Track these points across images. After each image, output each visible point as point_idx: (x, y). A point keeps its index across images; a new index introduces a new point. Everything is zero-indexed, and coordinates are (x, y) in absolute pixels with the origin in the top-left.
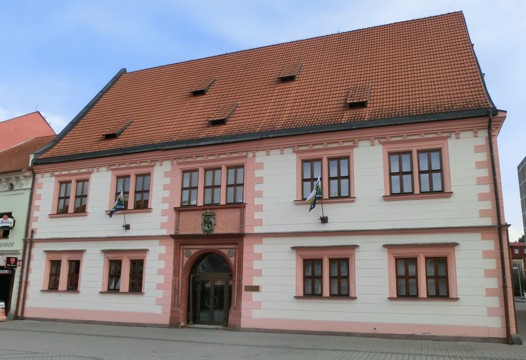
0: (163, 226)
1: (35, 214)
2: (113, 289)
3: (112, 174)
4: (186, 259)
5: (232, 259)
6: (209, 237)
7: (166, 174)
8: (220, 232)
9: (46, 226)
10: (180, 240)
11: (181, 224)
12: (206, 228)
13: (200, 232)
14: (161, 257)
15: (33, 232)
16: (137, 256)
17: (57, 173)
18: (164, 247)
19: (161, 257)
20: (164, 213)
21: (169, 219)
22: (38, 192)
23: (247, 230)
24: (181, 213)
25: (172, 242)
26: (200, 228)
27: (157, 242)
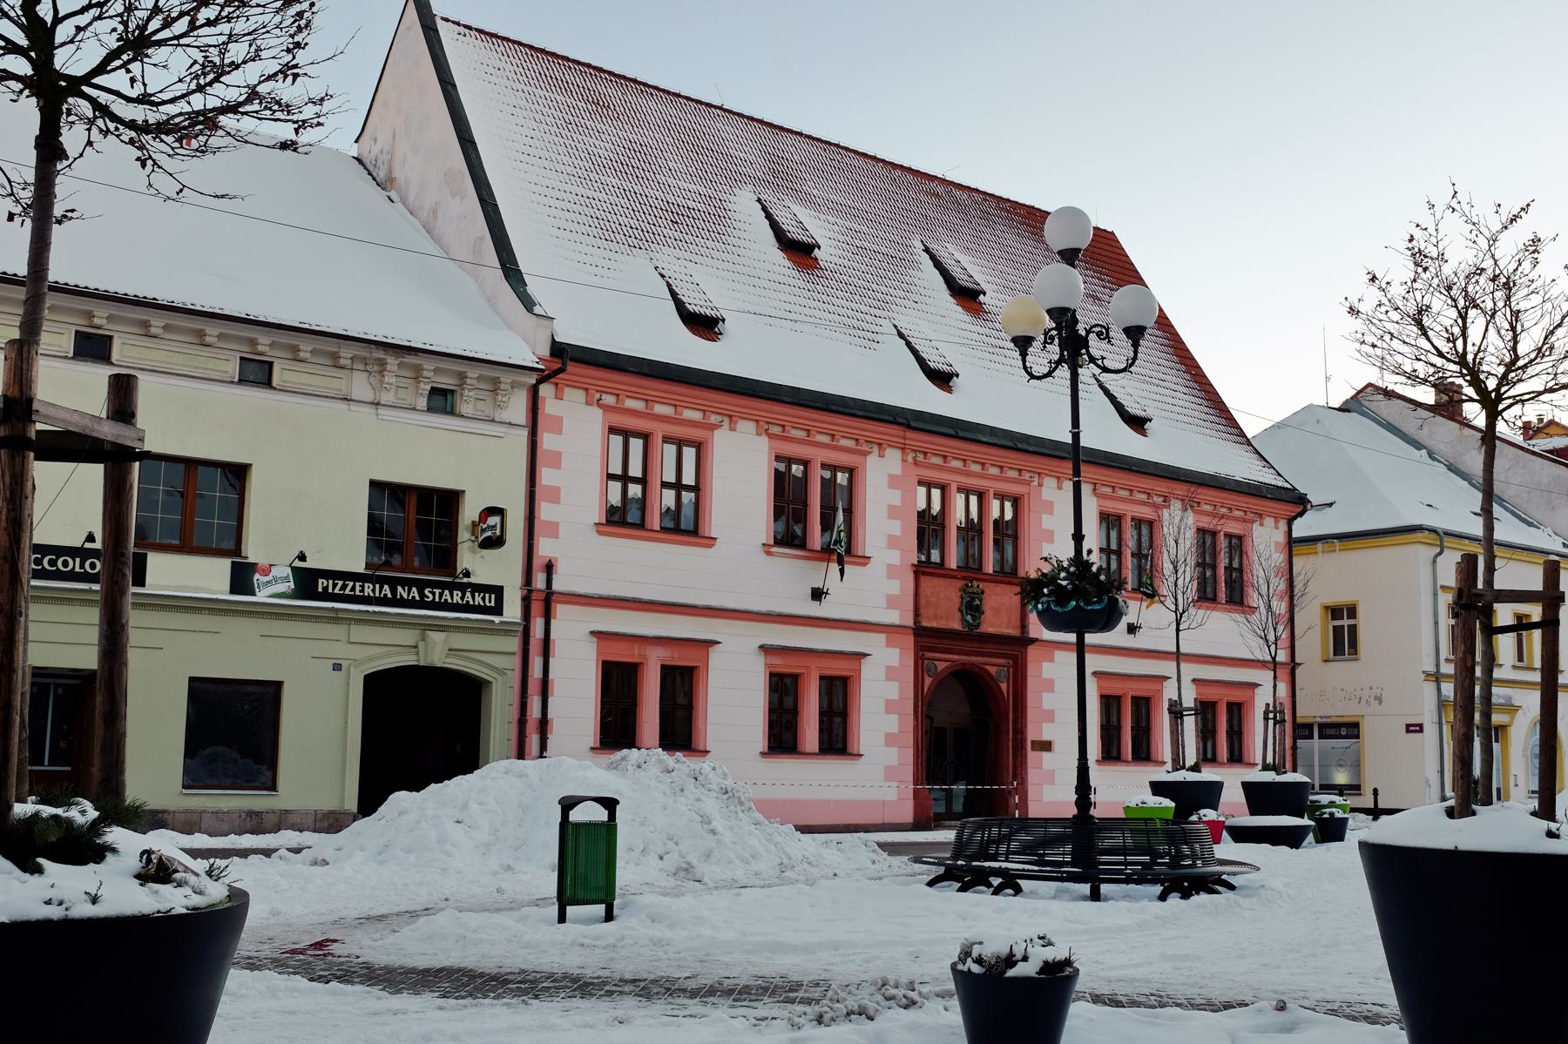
0: (891, 602)
1: (545, 511)
2: (782, 740)
3: (770, 447)
4: (928, 681)
5: (1004, 686)
6: (971, 638)
7: (893, 482)
8: (991, 630)
9: (585, 556)
10: (925, 639)
11: (922, 602)
12: (969, 618)
13: (956, 625)
14: (891, 673)
15: (549, 568)
16: (837, 668)
17: (609, 400)
18: (896, 651)
19: (891, 673)
20: (892, 572)
21: (901, 587)
22: (547, 441)
23: (1032, 635)
24: (923, 579)
25: (910, 641)
26: (958, 615)
27: (882, 638)
